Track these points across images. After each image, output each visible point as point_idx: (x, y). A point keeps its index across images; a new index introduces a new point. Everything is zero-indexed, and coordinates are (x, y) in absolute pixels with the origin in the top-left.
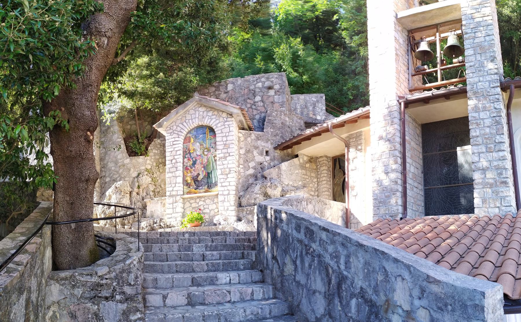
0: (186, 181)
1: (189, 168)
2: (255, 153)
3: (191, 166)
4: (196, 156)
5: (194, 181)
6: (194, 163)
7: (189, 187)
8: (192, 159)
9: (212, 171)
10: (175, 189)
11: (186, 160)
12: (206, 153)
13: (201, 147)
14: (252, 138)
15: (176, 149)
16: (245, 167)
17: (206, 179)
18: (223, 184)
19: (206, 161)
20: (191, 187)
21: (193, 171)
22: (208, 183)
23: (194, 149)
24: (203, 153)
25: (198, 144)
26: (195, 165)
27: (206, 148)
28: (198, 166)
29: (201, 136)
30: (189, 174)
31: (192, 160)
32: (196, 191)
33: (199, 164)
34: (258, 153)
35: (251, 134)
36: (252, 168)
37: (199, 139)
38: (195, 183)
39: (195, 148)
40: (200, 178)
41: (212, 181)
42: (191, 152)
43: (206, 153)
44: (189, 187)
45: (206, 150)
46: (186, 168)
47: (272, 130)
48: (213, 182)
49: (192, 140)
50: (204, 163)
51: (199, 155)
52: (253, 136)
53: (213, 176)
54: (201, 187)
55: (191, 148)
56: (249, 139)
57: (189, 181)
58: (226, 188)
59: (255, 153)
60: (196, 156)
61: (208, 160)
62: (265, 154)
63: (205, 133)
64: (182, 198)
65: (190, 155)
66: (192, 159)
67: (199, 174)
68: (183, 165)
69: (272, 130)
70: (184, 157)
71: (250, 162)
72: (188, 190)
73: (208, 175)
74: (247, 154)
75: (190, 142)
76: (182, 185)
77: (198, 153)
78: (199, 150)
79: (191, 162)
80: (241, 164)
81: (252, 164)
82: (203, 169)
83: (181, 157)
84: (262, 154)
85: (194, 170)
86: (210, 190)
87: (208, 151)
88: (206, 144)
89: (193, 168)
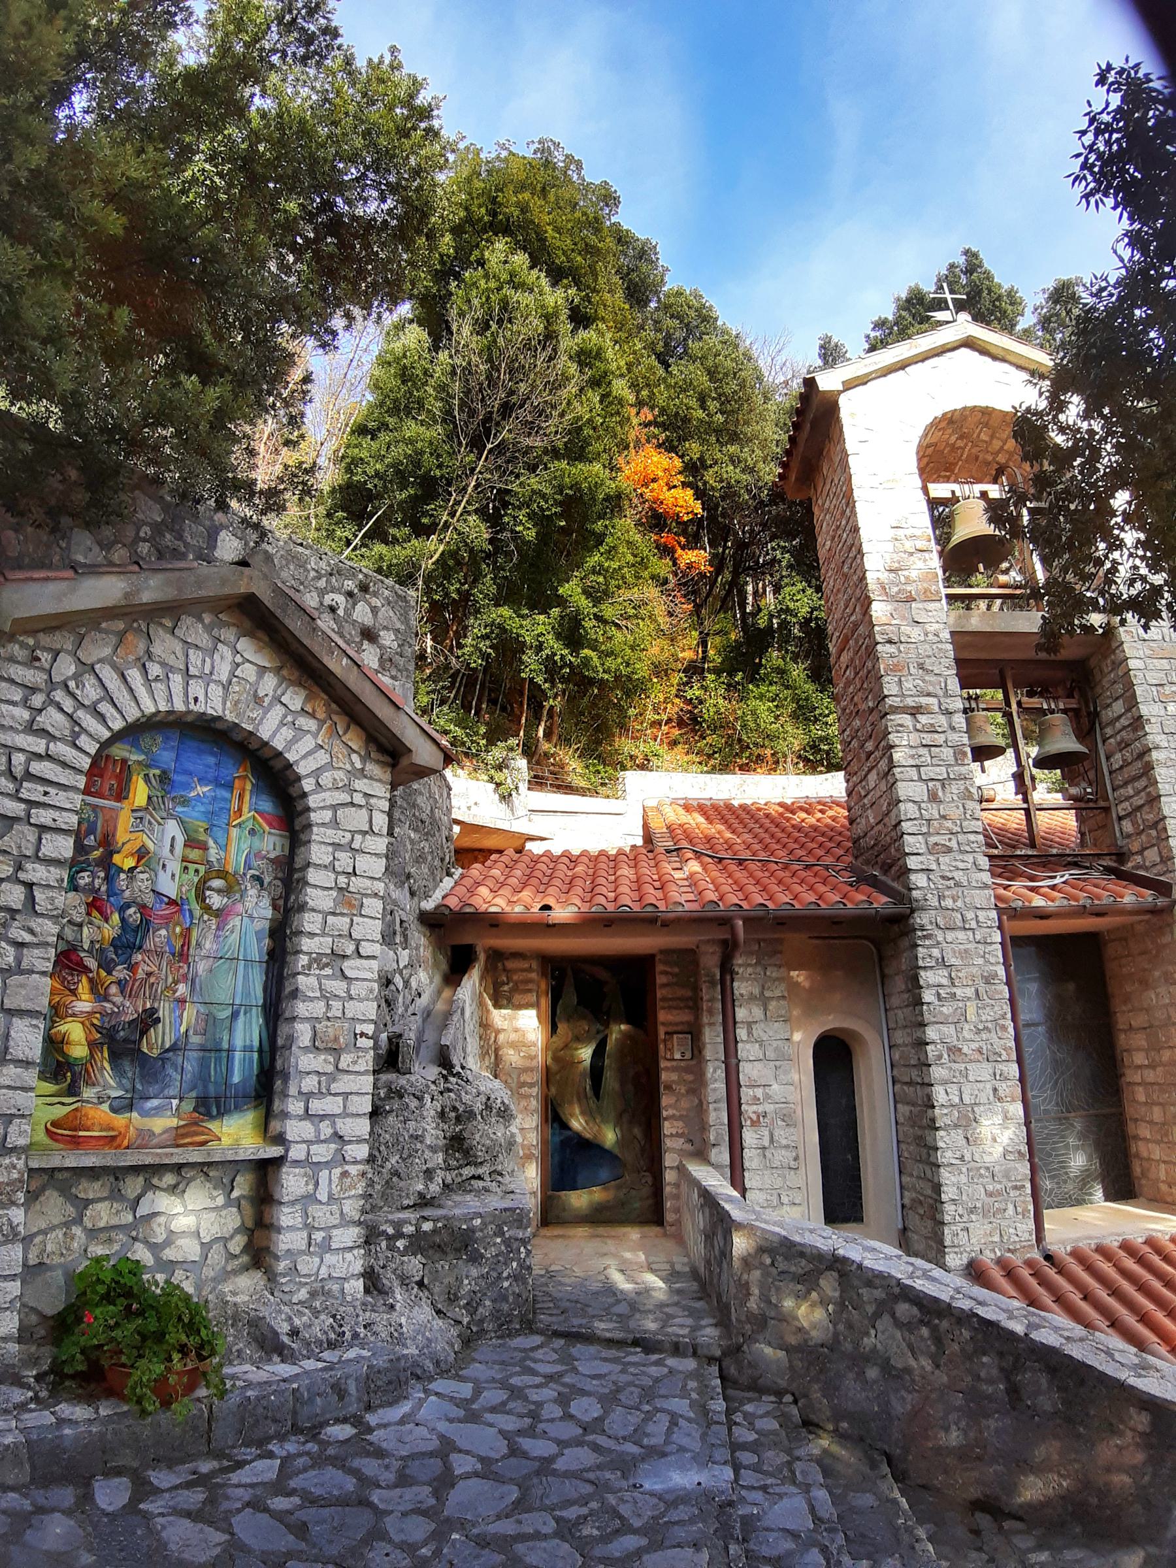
1: (91, 963)
3: (102, 950)
4: (149, 899)
7: (73, 1091)
8: (122, 909)
13: (194, 854)
15: (43, 816)
18: (316, 1106)
20: (88, 1093)
21: (114, 989)
23: (142, 854)
24: (201, 897)
25: (172, 829)
26: (138, 957)
27: (222, 874)
29: (202, 790)
30: (84, 1004)
31: (116, 918)
32: (120, 1120)
33: (160, 955)
37: (185, 802)
39: (150, 846)
42: (117, 859)
43: (216, 901)
45: (217, 883)
49: (140, 793)
51: (172, 902)
54: (155, 1102)
57: (79, 1051)
58: (326, 1129)
65: (108, 879)
66: (122, 909)
72: (60, 1112)
75: (121, 794)
77: (170, 889)
78: (174, 866)
79: (110, 930)
85: (120, 983)
87: (226, 892)
88: (225, 847)
89: (120, 972)
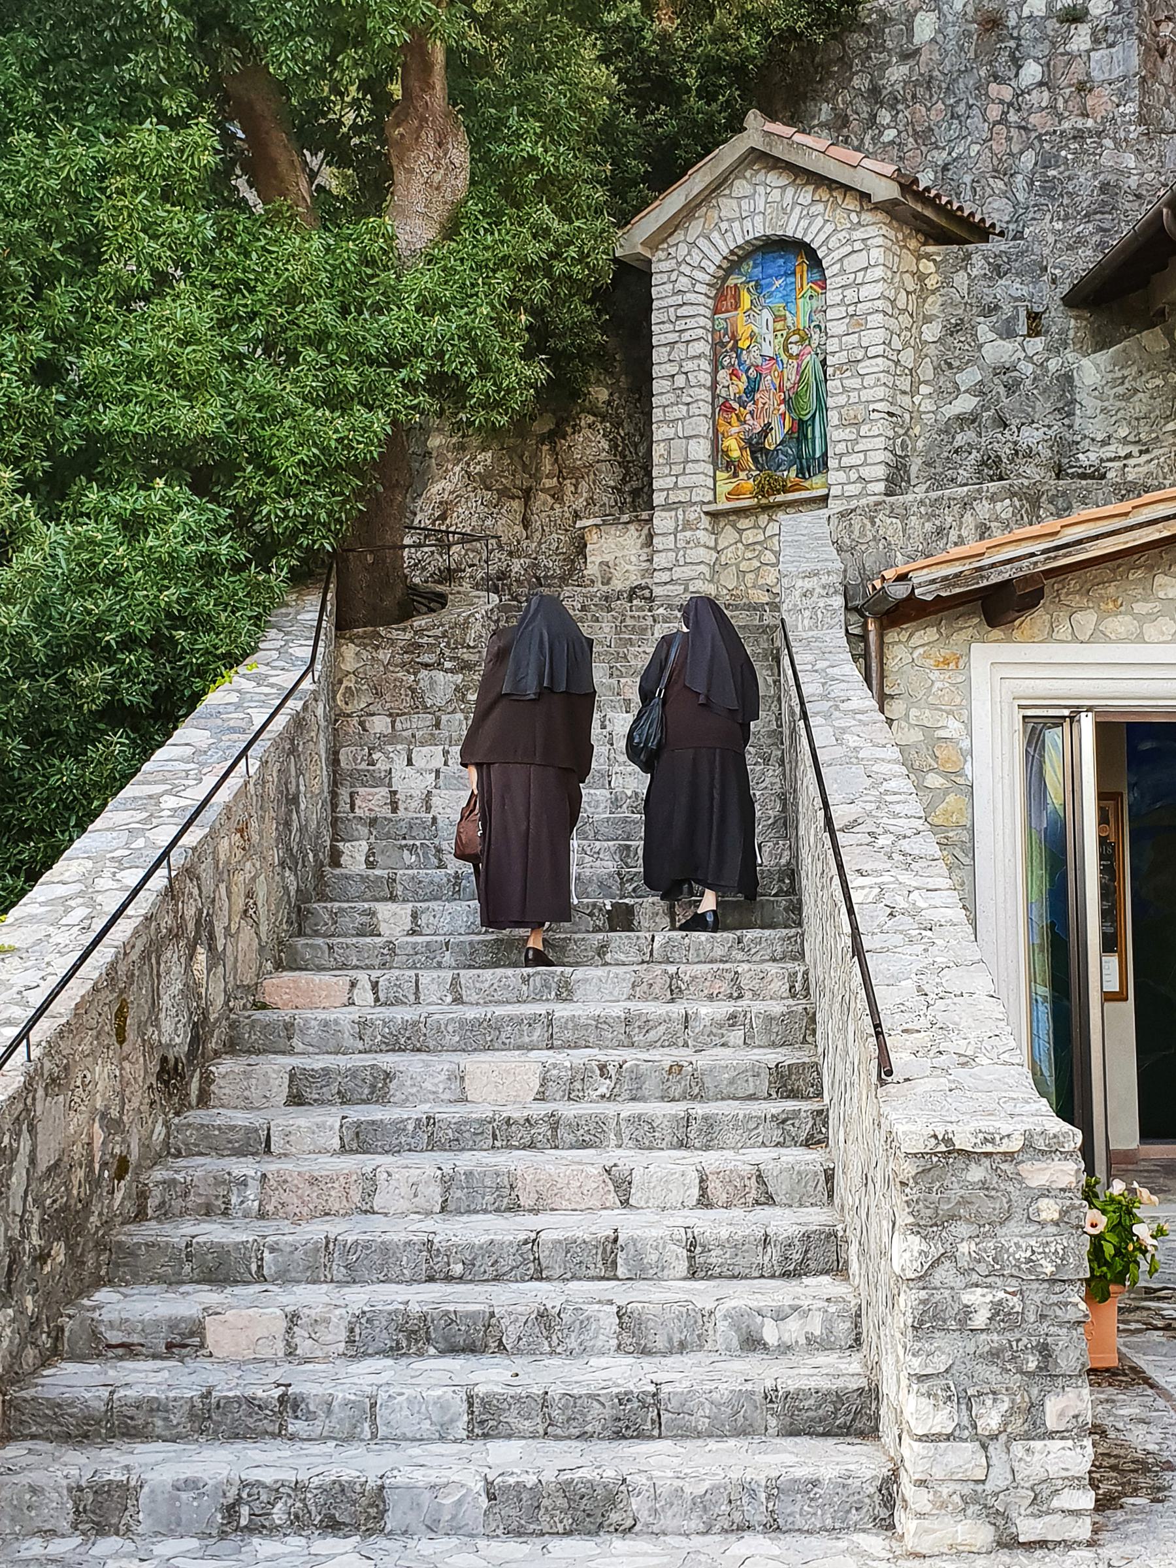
0: (726, 453)
1: (736, 406)
2: (984, 331)
4: (759, 361)
5: (752, 453)
6: (752, 389)
8: (747, 371)
9: (814, 416)
10: (681, 482)
11: (723, 375)
12: (794, 350)
13: (779, 325)
14: (975, 272)
16: (940, 391)
17: (793, 444)
18: (846, 461)
19: (794, 378)
20: (742, 475)
21: (748, 417)
22: (800, 458)
24: (786, 350)
25: (766, 314)
26: (757, 396)
28: (768, 398)
29: (777, 284)
31: (744, 378)
33: (768, 391)
34: (993, 329)
35: (968, 256)
36: (966, 391)
38: (755, 460)
39: (756, 330)
40: (771, 443)
41: (814, 450)
42: (740, 344)
44: (735, 475)
45: (795, 338)
46: (722, 407)
47: (1058, 226)
48: (818, 455)
49: (746, 299)
50: (788, 385)
52: (978, 266)
53: (817, 434)
55: (743, 330)
56: (961, 279)
57: (735, 454)
58: (854, 476)
59: (984, 331)
60: (759, 361)
61: (800, 374)
62: (1022, 328)
63: (794, 273)
64: (707, 513)
67: (767, 430)
68: (715, 396)
69: (1058, 226)
70: (716, 365)
71: (960, 370)
72: (731, 487)
73: (800, 431)
74: (949, 339)
76: (709, 469)
77: (768, 351)
78: (770, 337)
79: (742, 385)
80: (926, 382)
81: (969, 377)
82: (782, 407)
83: (705, 365)
84: (1008, 332)
85: (751, 413)
86: (807, 484)
88: (795, 315)
89: (750, 406)
